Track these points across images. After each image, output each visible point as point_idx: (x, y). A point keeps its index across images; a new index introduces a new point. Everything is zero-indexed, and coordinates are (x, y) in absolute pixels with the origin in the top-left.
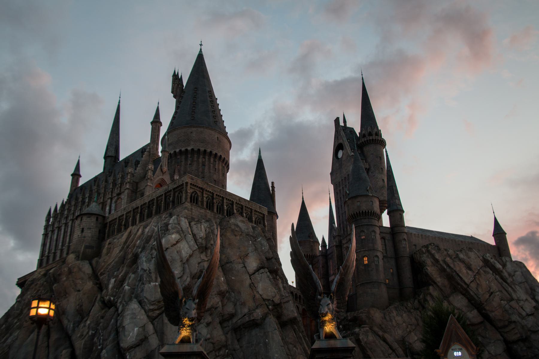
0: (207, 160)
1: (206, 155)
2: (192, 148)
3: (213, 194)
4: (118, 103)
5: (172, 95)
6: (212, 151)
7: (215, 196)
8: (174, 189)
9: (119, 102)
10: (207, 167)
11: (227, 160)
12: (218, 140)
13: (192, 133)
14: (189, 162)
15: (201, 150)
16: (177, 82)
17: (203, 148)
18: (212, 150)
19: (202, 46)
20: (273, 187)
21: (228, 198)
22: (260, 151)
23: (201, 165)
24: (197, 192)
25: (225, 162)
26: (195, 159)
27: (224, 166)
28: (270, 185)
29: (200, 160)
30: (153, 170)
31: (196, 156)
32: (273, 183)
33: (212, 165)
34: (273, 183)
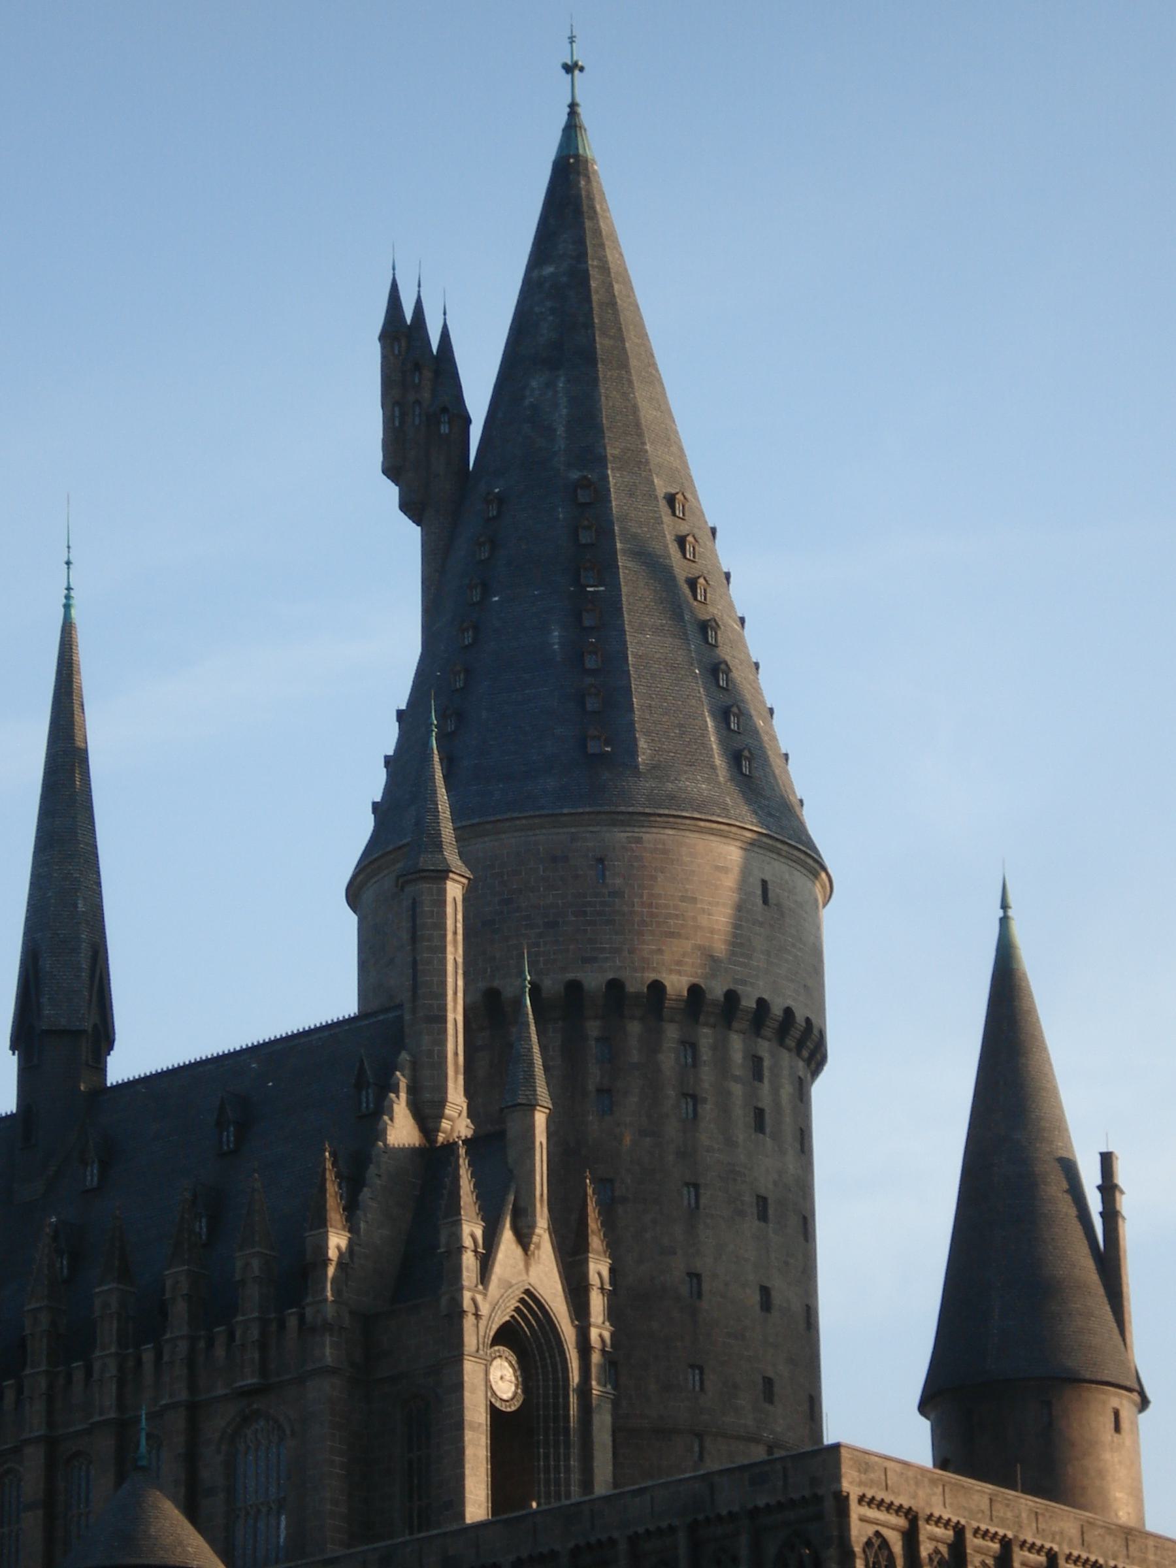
0: (706, 1054)
1: (702, 1019)
2: (611, 976)
3: (959, 1531)
4: (62, 610)
5: (391, 492)
6: (740, 988)
7: (972, 1542)
8: (754, 1513)
9: (67, 607)
10: (708, 1107)
11: (808, 1020)
12: (765, 901)
13: (601, 860)
14: (594, 1076)
15: (669, 990)
16: (426, 395)
17: (679, 973)
18: (736, 981)
19: (577, 72)
20: (1108, 1189)
21: (1030, 1540)
22: (1005, 906)
23: (671, 1093)
24: (885, 1544)
25: (797, 1034)
26: (635, 1057)
27: (801, 1074)
28: (1090, 1178)
29: (668, 1061)
30: (480, 1250)
31: (634, 1028)
32: (1107, 1159)
33: (737, 1089)
34: (1107, 1159)
